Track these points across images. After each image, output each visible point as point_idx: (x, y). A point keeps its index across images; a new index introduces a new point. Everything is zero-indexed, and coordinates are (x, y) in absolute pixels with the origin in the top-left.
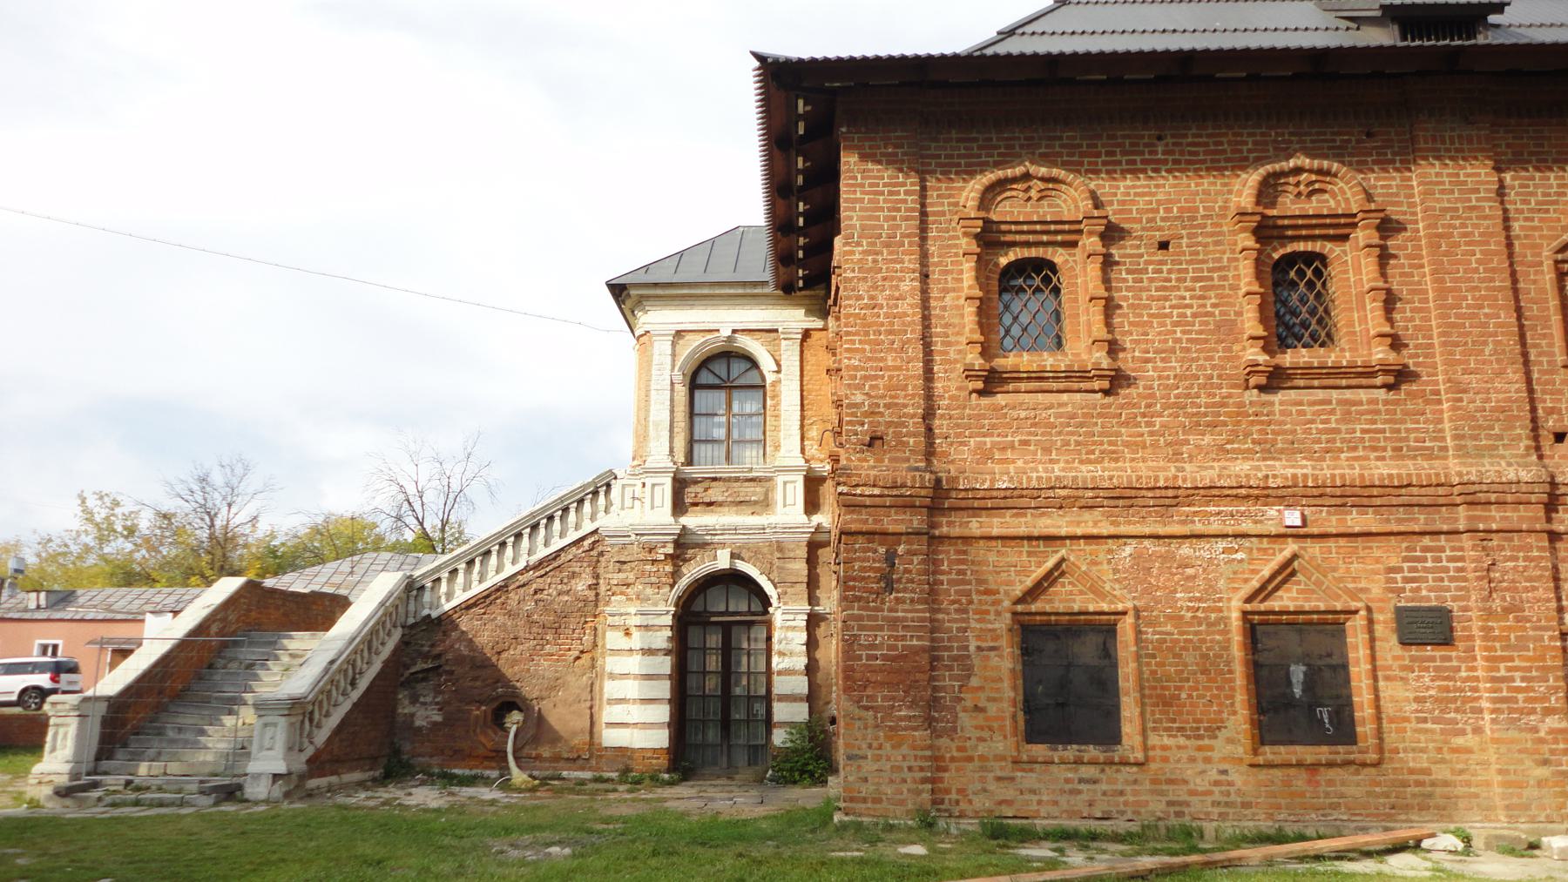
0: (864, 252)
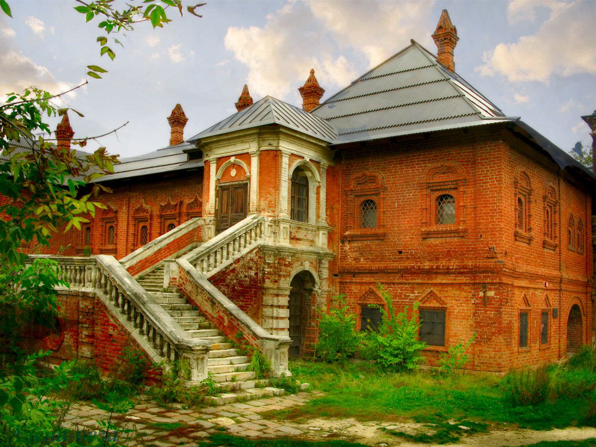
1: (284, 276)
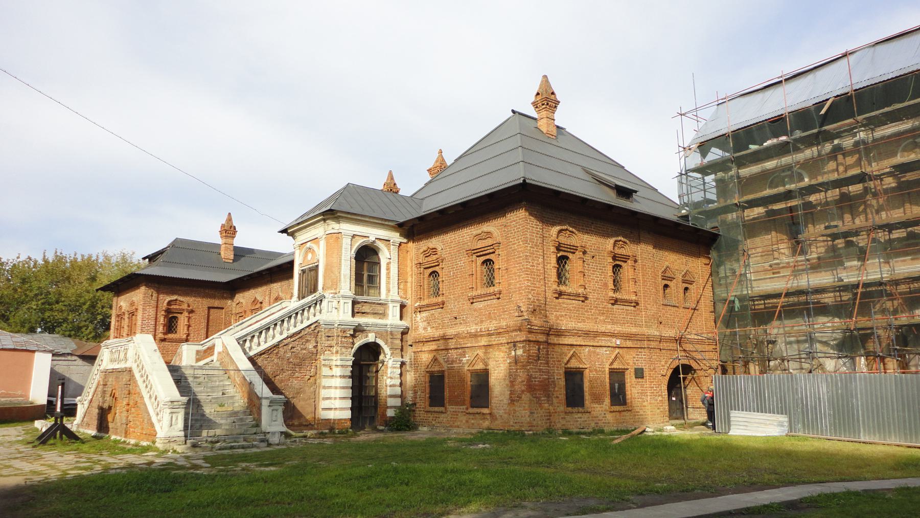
0: (530, 247)
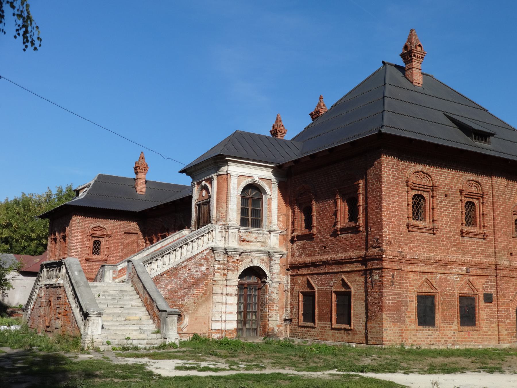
0: (386, 187)
1: (232, 270)
